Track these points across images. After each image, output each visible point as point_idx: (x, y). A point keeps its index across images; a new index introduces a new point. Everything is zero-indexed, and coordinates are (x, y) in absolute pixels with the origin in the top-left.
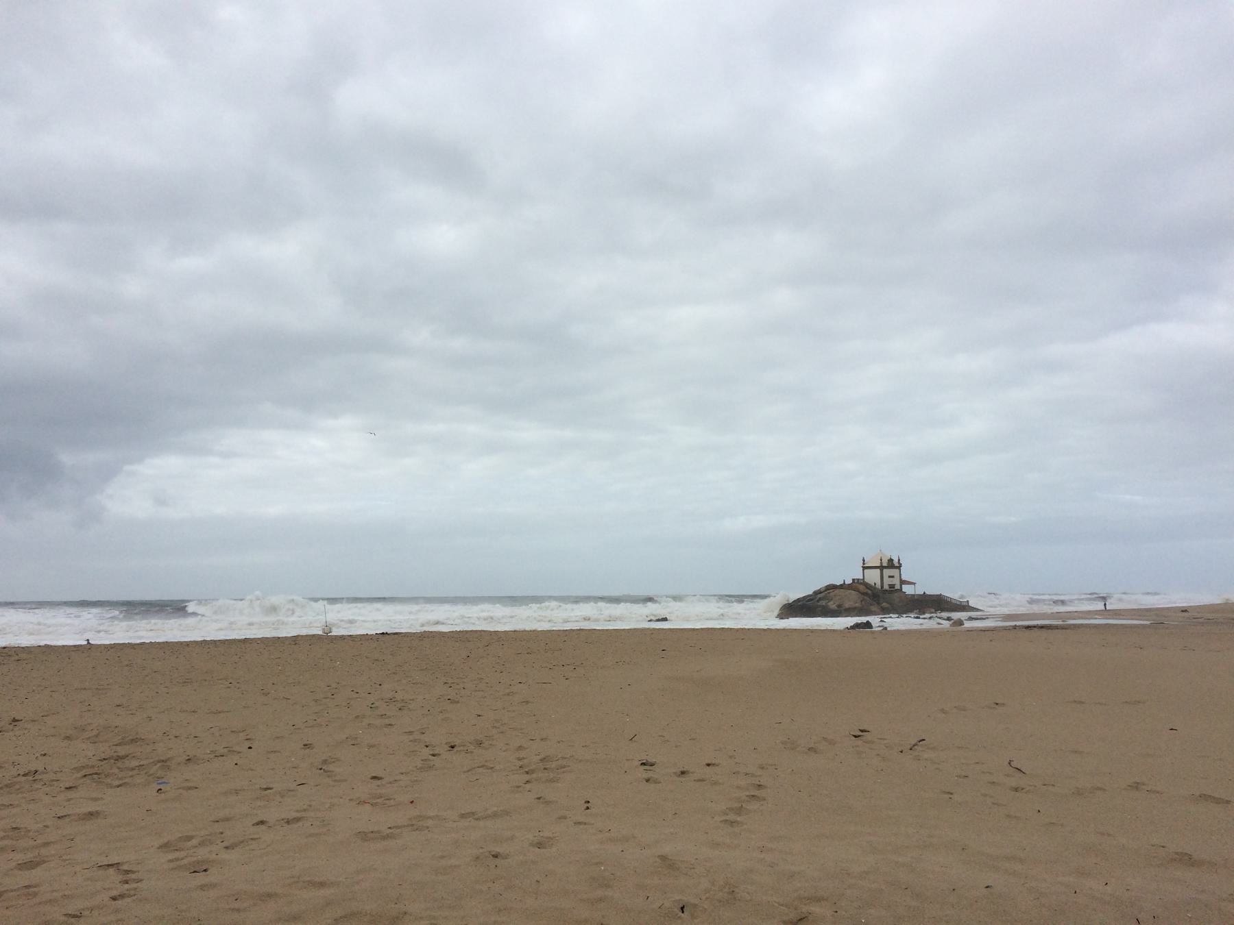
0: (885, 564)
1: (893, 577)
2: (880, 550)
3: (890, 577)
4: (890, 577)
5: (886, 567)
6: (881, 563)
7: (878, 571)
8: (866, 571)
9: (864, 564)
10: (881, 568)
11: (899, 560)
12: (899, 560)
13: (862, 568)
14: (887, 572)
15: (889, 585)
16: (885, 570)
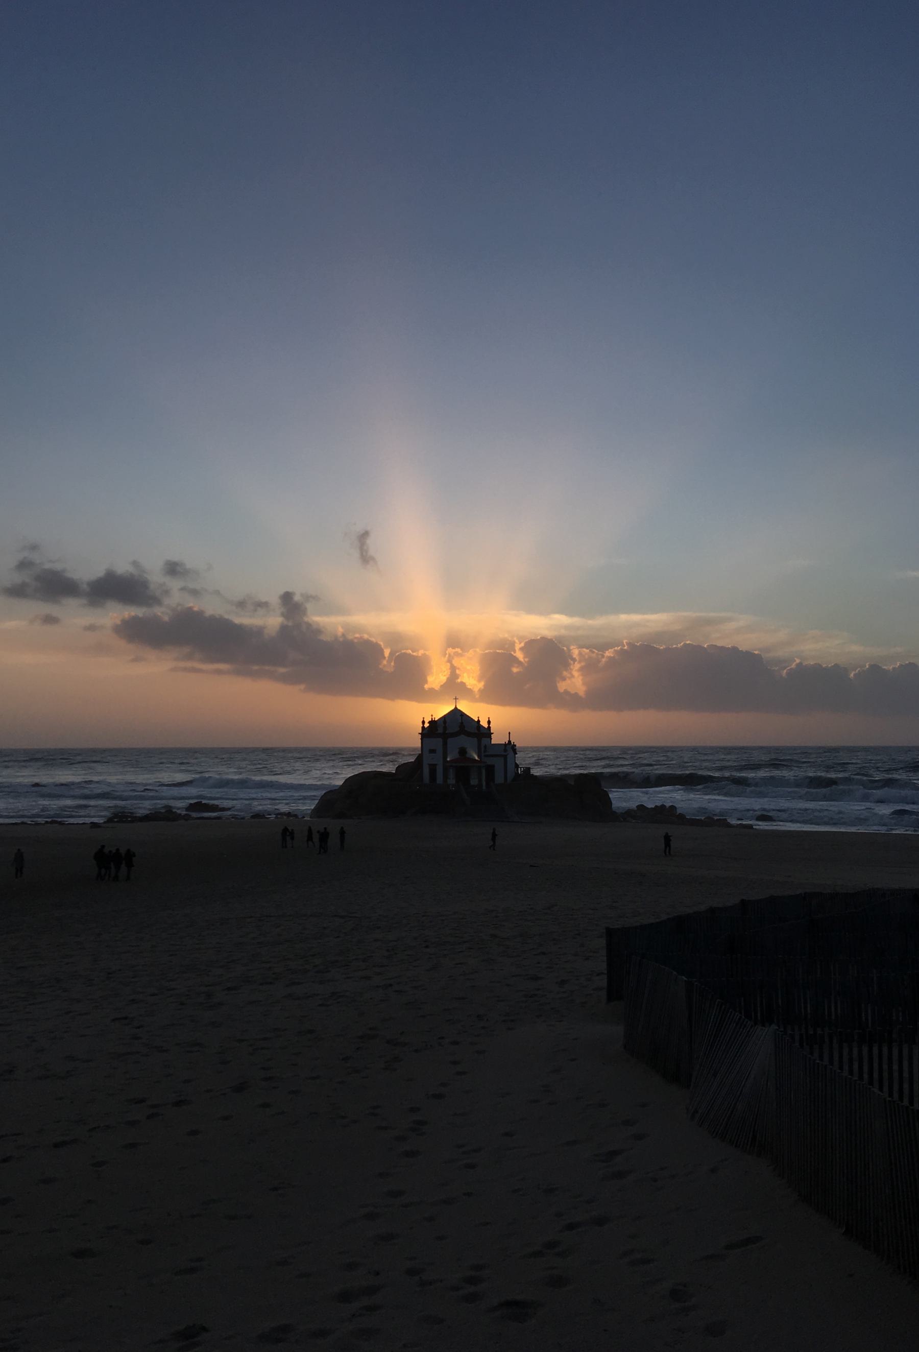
2: (456, 706)
15: (429, 765)
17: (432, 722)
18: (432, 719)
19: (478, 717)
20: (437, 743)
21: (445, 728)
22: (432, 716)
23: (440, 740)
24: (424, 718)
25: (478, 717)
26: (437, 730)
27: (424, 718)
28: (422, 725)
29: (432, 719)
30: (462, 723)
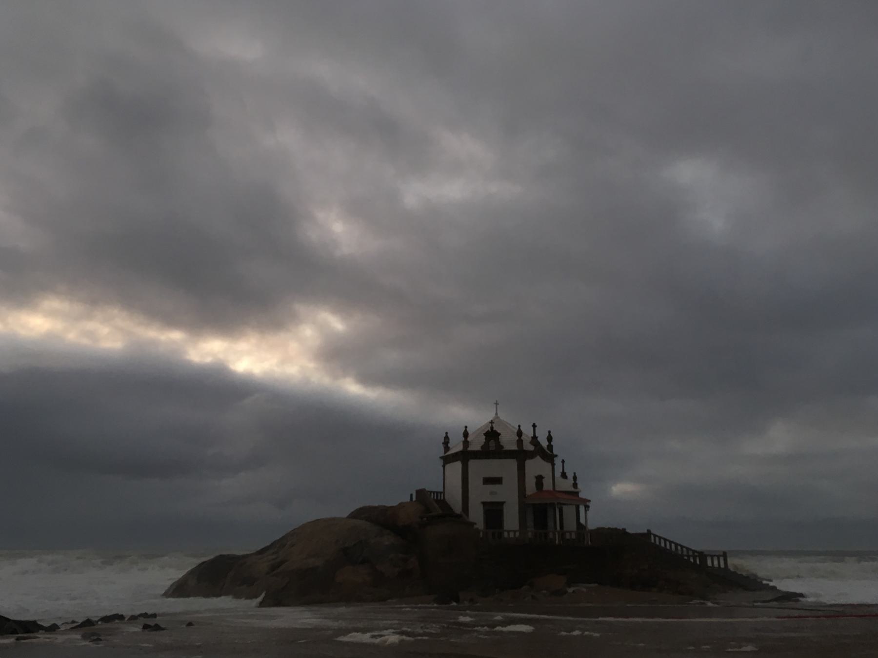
0: (476, 444)
1: (497, 481)
2: (497, 414)
3: (488, 481)
4: (488, 481)
5: (476, 455)
6: (466, 443)
7: (458, 466)
8: (447, 466)
9: (447, 448)
10: (465, 456)
11: (550, 439)
12: (550, 439)
13: (441, 462)
14: (479, 468)
15: (484, 503)
16: (473, 464)
17: (492, 435)
18: (492, 428)
19: (549, 432)
20: (507, 469)
21: (520, 442)
22: (492, 422)
23: (512, 465)
24: (466, 427)
25: (549, 432)
26: (502, 447)
27: (466, 427)
28: (463, 439)
29: (492, 428)
30: (535, 438)
